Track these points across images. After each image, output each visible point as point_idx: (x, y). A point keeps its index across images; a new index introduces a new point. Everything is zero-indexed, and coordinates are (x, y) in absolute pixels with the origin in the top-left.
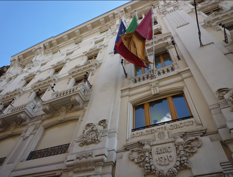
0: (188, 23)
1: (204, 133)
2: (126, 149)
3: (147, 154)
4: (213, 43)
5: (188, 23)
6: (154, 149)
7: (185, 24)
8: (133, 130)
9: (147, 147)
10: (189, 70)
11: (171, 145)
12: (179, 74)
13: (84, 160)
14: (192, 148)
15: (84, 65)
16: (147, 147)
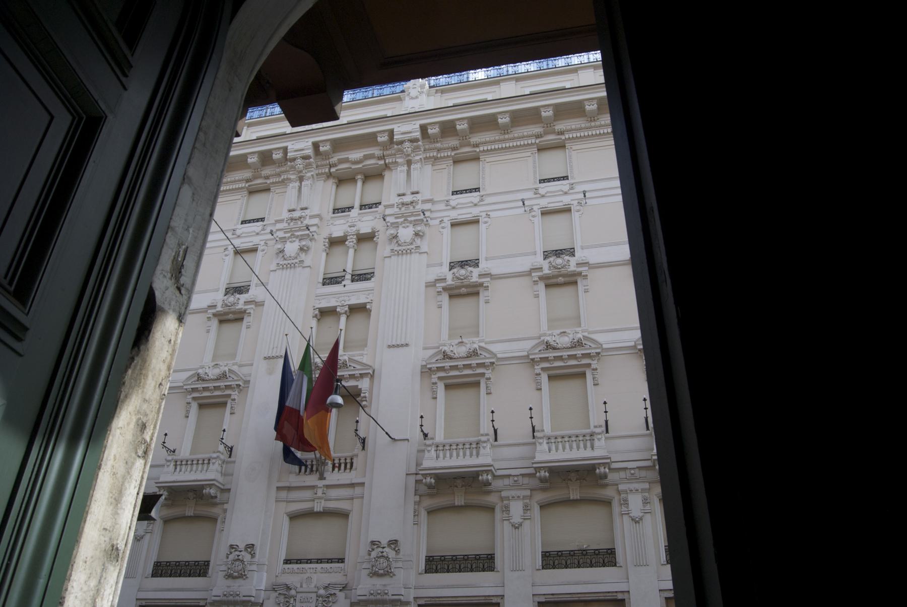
0: (407, 345)
1: (344, 588)
2: (274, 590)
3: (292, 601)
4: (408, 440)
5: (407, 345)
6: (299, 596)
7: (402, 345)
8: (287, 561)
9: (293, 592)
10: (362, 484)
11: (314, 596)
12: (352, 485)
13: (231, 598)
14: (329, 602)
15: (217, 379)
16: (293, 592)
